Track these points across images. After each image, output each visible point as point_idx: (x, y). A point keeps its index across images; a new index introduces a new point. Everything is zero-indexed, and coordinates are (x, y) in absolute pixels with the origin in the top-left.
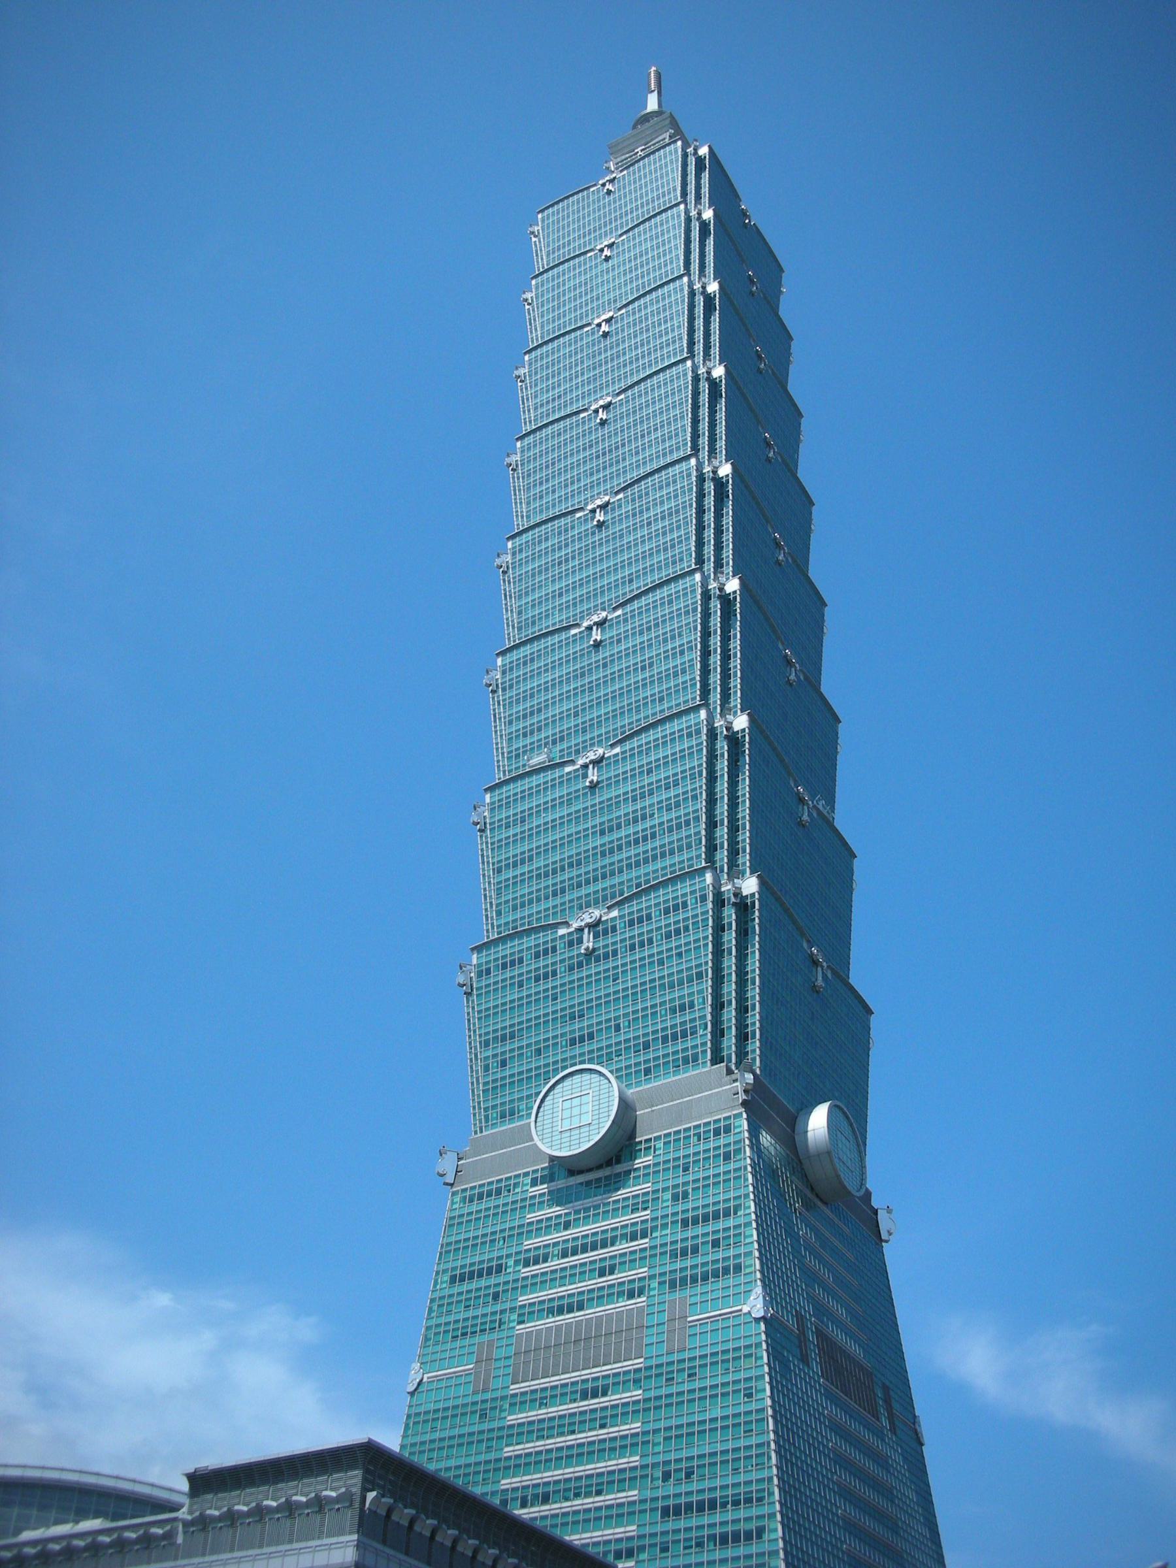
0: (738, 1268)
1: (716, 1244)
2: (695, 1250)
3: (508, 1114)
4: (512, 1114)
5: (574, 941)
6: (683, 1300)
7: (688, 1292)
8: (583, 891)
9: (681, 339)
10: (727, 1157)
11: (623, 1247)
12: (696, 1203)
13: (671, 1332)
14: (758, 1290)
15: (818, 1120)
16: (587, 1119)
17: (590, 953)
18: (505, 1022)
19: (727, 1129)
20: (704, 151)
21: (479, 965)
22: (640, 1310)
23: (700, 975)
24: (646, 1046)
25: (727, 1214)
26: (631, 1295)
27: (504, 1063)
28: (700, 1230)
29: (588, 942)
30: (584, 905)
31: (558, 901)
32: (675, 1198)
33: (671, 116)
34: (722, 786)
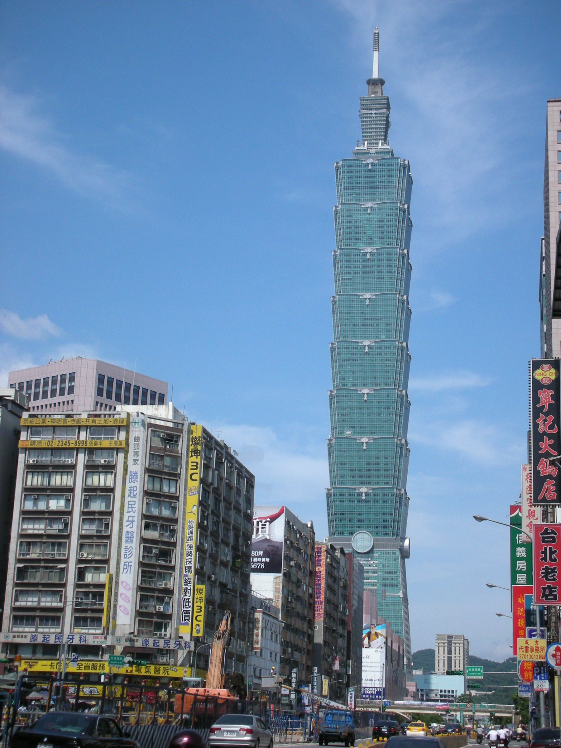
0: (397, 586)
1: (392, 579)
2: (388, 579)
3: (341, 534)
4: (343, 533)
5: (360, 494)
6: (385, 590)
7: (386, 588)
8: (361, 479)
9: (395, 278)
10: (395, 560)
11: (370, 574)
12: (388, 569)
13: (382, 596)
14: (401, 591)
15: (406, 543)
16: (365, 544)
17: (364, 500)
18: (340, 510)
19: (395, 553)
20: (406, 162)
21: (334, 492)
22: (376, 590)
23: (391, 514)
24: (377, 527)
25: (395, 573)
26: (373, 585)
27: (341, 521)
28: (389, 575)
29: (364, 498)
30: (362, 483)
31: (354, 479)
32: (383, 566)
33: (388, 99)
34: (398, 461)
